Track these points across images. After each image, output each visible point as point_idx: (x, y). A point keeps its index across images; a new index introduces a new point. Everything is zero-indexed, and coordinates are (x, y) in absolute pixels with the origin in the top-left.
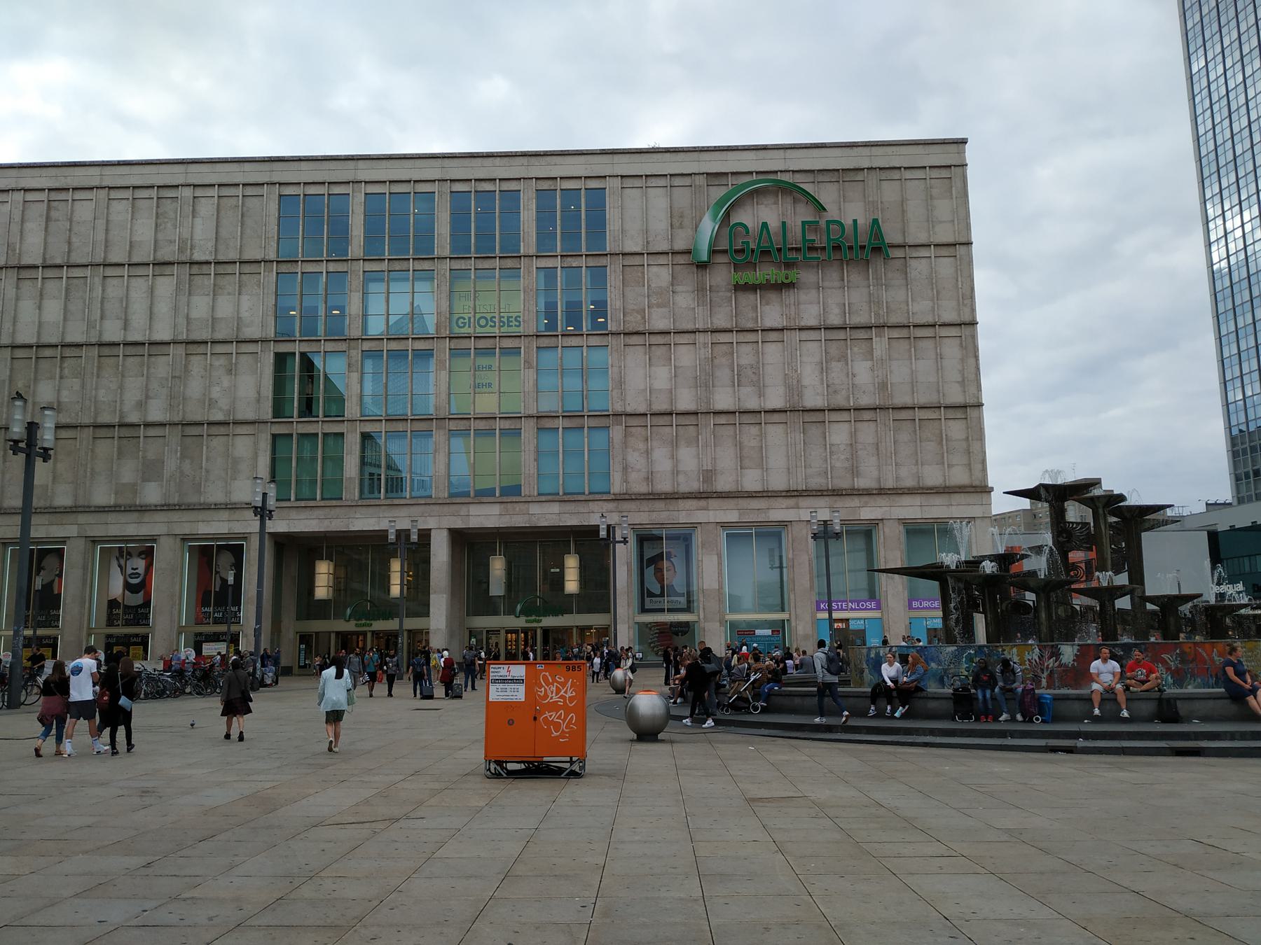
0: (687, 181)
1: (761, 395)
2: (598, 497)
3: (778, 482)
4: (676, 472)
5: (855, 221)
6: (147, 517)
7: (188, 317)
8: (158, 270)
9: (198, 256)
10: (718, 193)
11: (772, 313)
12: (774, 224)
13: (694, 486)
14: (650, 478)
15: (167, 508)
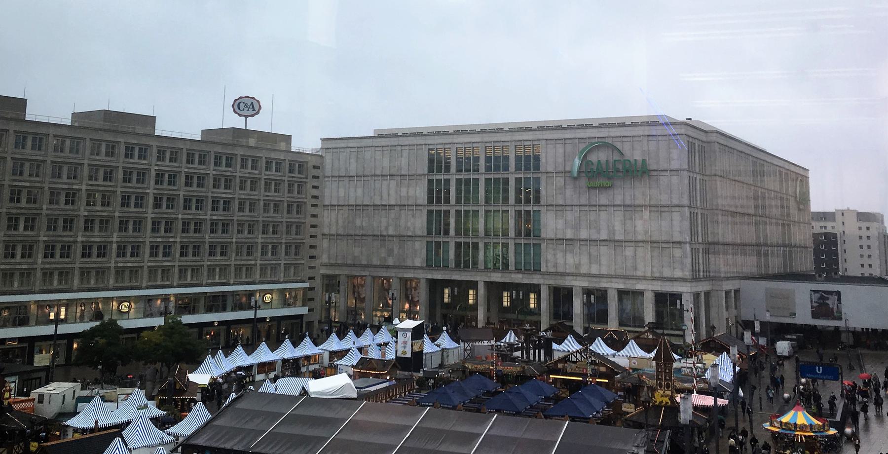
3: (604, 271)
8: (391, 178)
9: (403, 173)
11: (603, 199)
15: (394, 267)
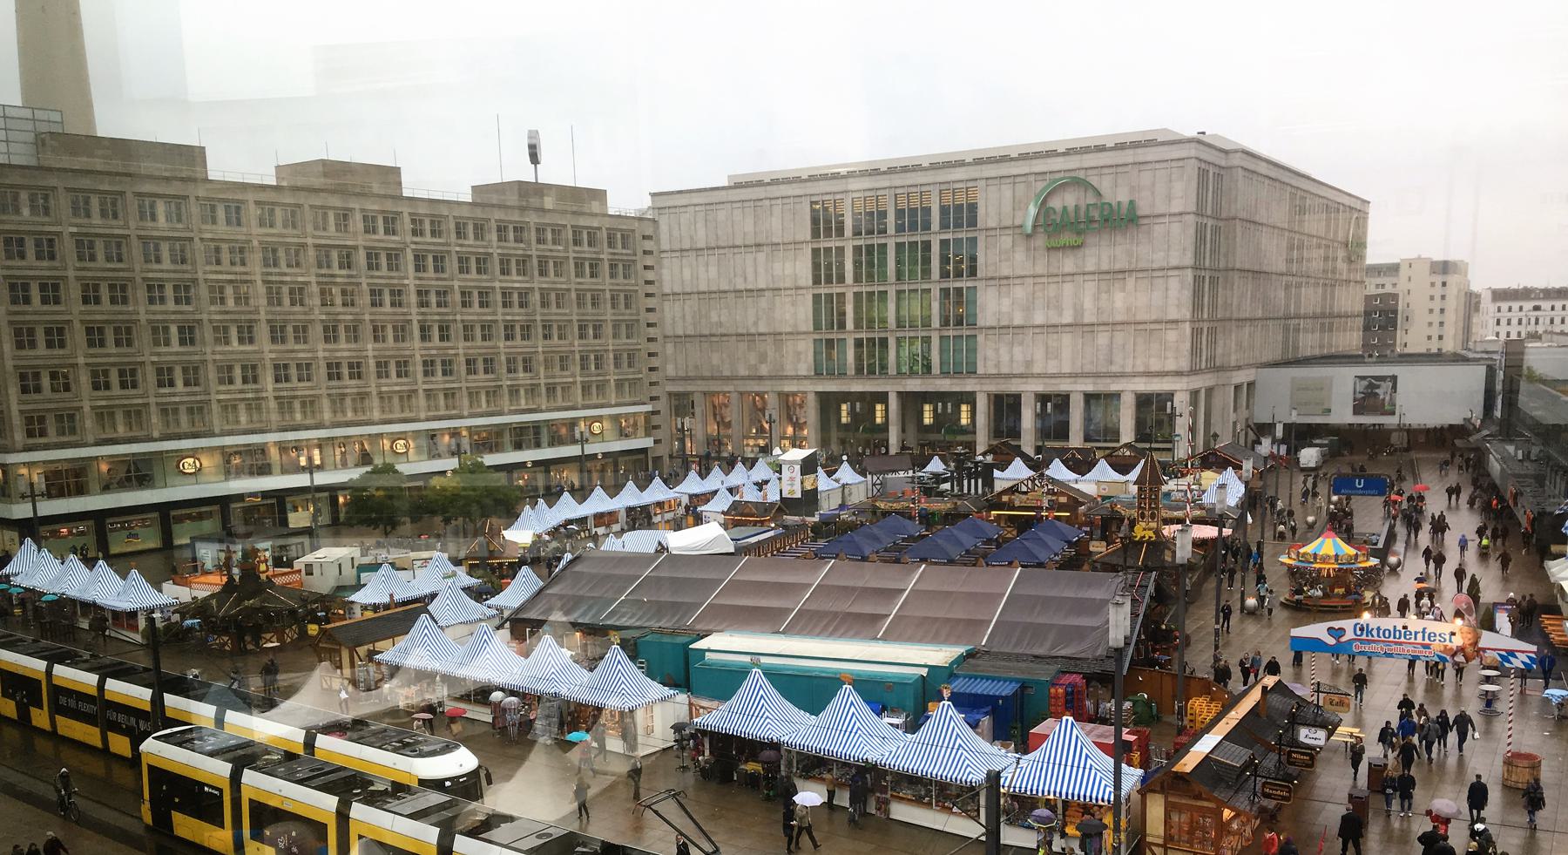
0: (1023, 179)
1: (1060, 315)
3: (1066, 369)
4: (1012, 360)
6: (762, 382)
7: (772, 276)
9: (775, 240)
10: (1040, 185)
11: (1068, 263)
12: (1071, 208)
14: (997, 365)
15: (771, 378)
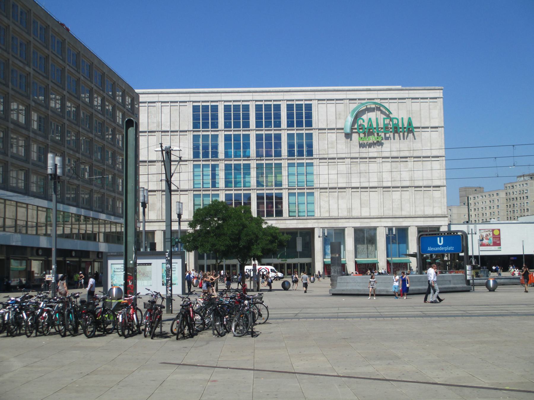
2: (311, 217)
3: (374, 214)
5: (402, 118)
10: (353, 106)
11: (373, 151)
13: (345, 214)
